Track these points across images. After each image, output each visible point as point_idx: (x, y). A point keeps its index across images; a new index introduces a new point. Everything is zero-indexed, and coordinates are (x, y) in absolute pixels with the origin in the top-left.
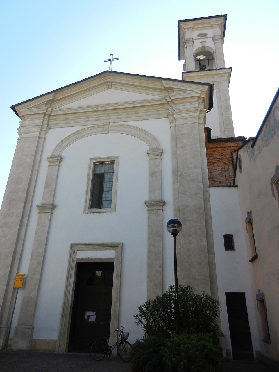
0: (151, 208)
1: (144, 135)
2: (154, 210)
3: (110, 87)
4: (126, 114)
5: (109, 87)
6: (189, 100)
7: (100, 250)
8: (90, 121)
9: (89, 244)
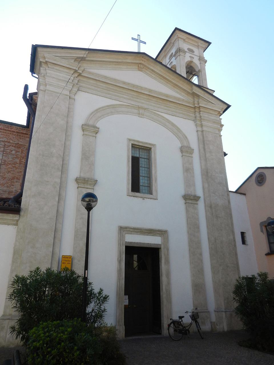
0: (188, 201)
1: (177, 132)
3: (140, 69)
4: (159, 105)
7: (147, 235)
8: (125, 98)
9: (138, 229)
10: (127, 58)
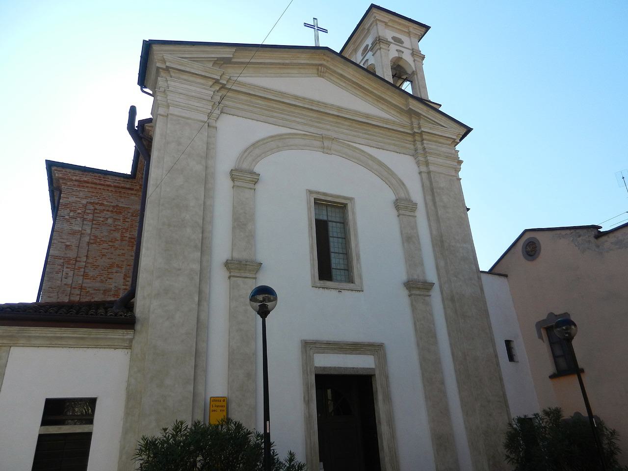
0: (414, 292)
2: (420, 295)
3: (320, 74)
5: (321, 75)
6: (441, 140)
7: (351, 353)
8: (298, 123)
10: (298, 57)
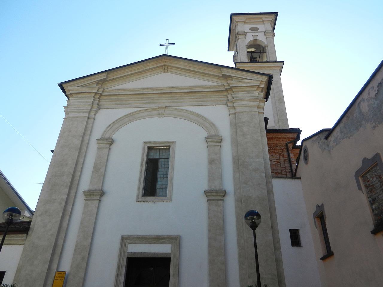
0: (210, 198)
1: (202, 121)
2: (214, 200)
4: (183, 99)
5: (165, 71)
6: (248, 89)
7: (154, 243)
8: (144, 103)
9: (143, 237)
10: (148, 66)
